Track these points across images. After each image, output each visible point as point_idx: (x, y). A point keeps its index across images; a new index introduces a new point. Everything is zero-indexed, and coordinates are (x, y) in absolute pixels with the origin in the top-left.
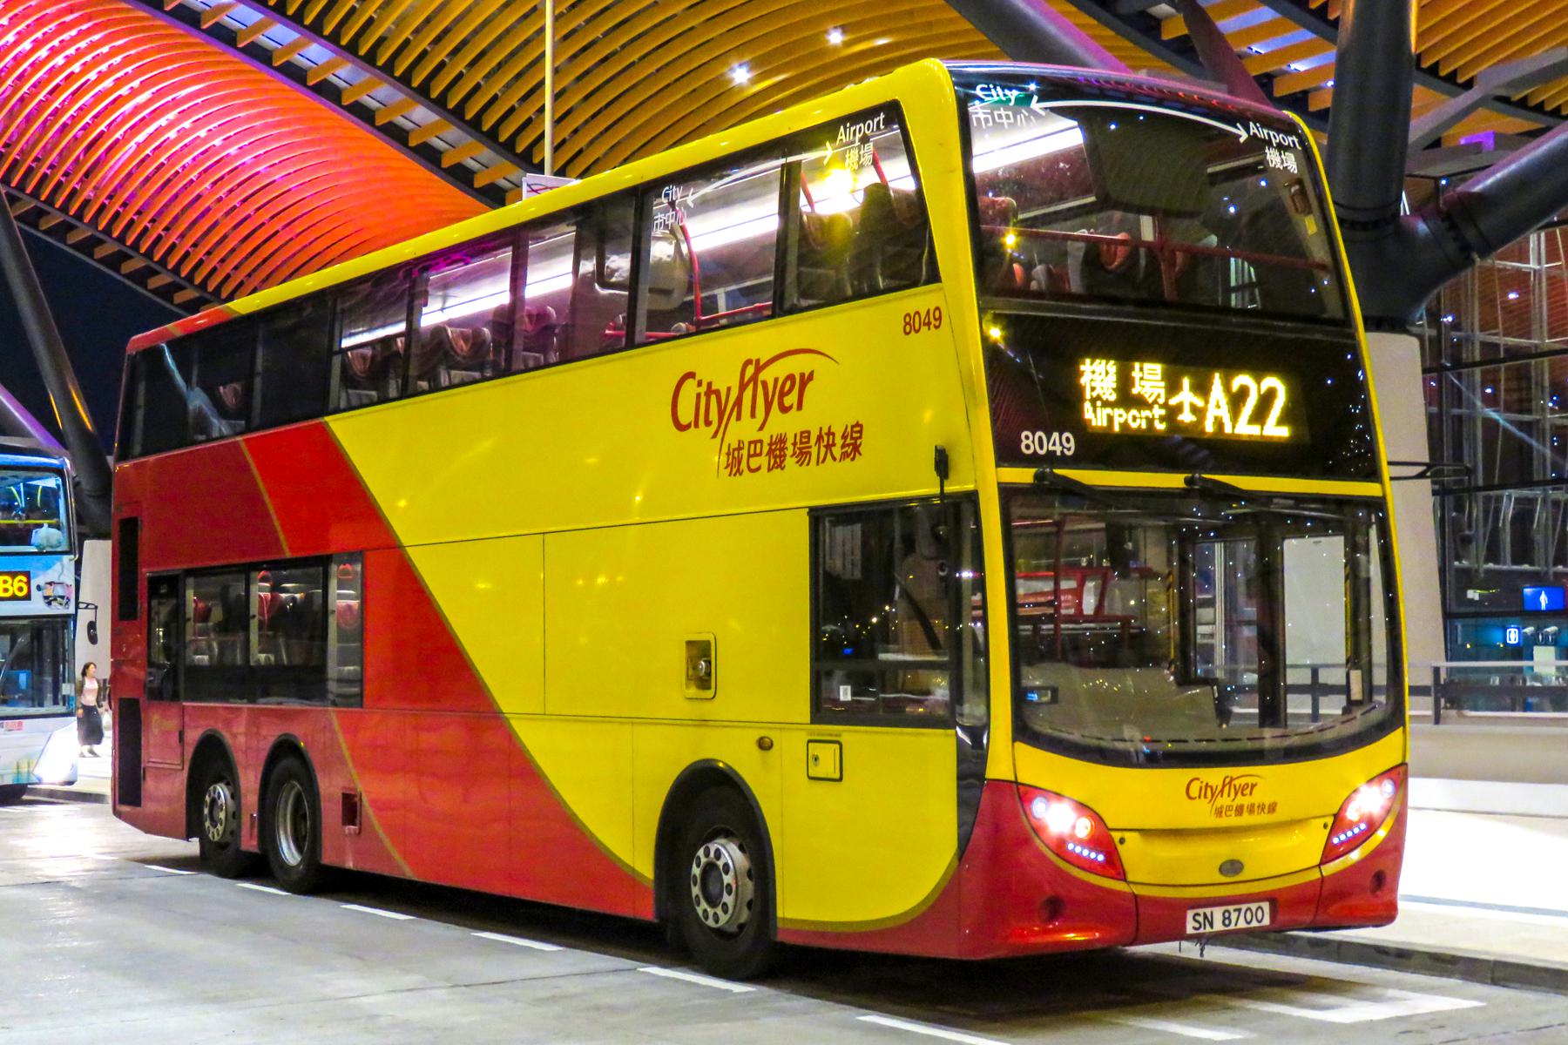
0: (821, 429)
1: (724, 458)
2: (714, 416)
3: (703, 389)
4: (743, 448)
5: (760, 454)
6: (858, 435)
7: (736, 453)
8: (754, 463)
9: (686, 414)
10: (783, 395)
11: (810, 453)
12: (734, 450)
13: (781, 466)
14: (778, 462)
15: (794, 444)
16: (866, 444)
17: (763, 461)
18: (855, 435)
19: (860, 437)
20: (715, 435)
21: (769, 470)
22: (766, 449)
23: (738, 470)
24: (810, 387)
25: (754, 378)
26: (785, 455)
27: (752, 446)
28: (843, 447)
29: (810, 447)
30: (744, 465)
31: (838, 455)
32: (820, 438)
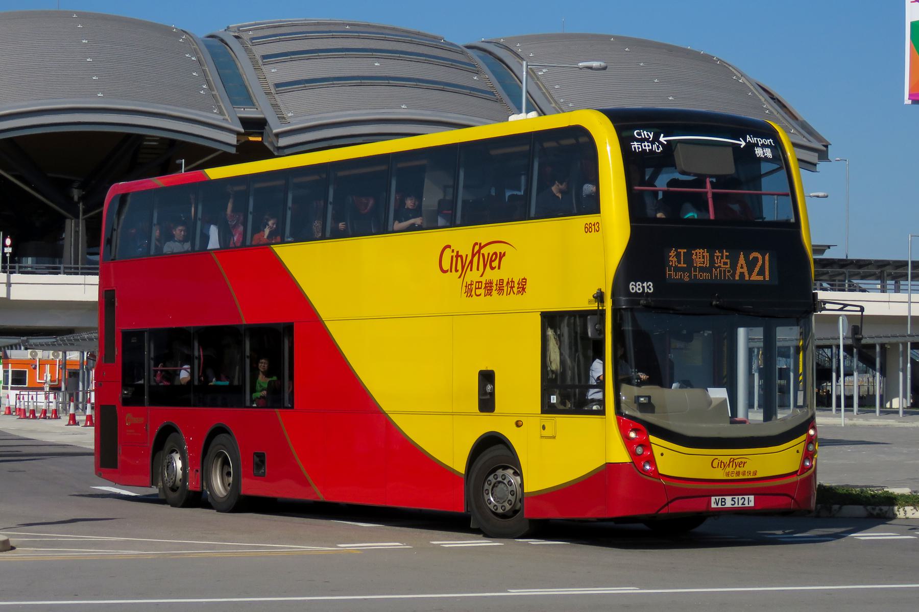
0: (508, 279)
1: (464, 288)
2: (459, 267)
3: (455, 254)
4: (473, 284)
5: (481, 288)
6: (524, 283)
7: (470, 287)
8: (478, 291)
9: (446, 266)
10: (492, 261)
11: (503, 289)
12: (469, 285)
13: (490, 294)
14: (489, 292)
15: (497, 285)
16: (528, 287)
17: (482, 291)
18: (524, 283)
19: (525, 285)
20: (460, 277)
21: (485, 296)
22: (484, 286)
23: (471, 294)
24: (504, 257)
25: (479, 252)
26: (492, 290)
27: (477, 284)
28: (518, 288)
29: (504, 287)
30: (473, 293)
31: (516, 293)
32: (508, 283)
